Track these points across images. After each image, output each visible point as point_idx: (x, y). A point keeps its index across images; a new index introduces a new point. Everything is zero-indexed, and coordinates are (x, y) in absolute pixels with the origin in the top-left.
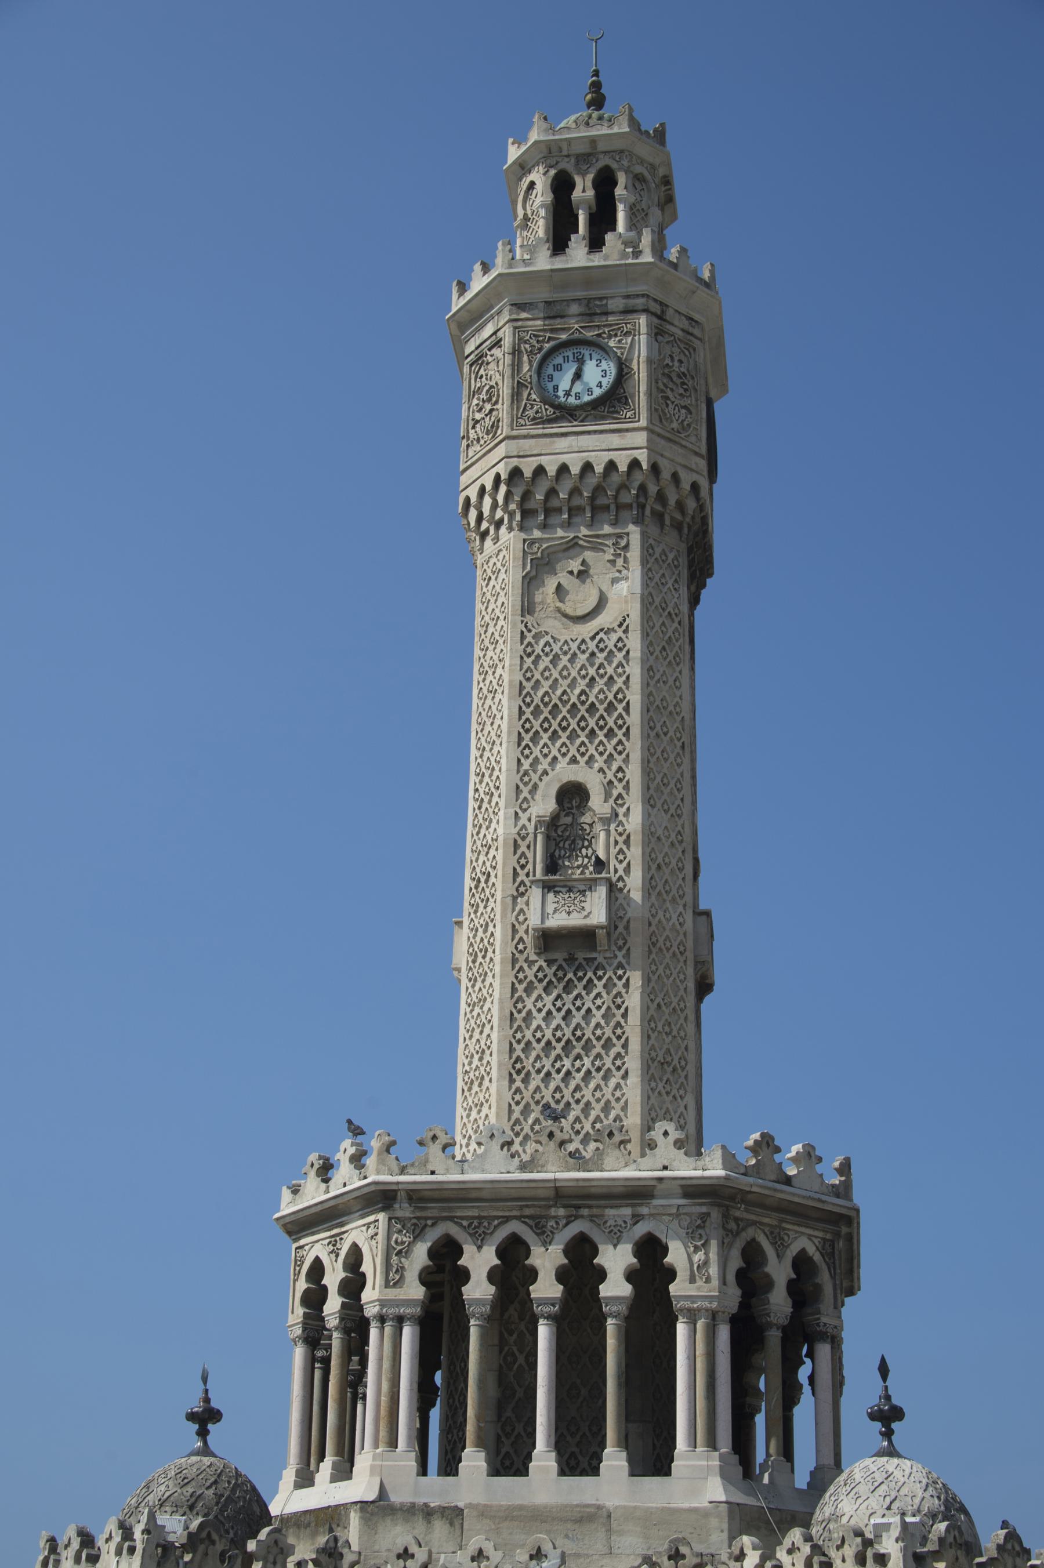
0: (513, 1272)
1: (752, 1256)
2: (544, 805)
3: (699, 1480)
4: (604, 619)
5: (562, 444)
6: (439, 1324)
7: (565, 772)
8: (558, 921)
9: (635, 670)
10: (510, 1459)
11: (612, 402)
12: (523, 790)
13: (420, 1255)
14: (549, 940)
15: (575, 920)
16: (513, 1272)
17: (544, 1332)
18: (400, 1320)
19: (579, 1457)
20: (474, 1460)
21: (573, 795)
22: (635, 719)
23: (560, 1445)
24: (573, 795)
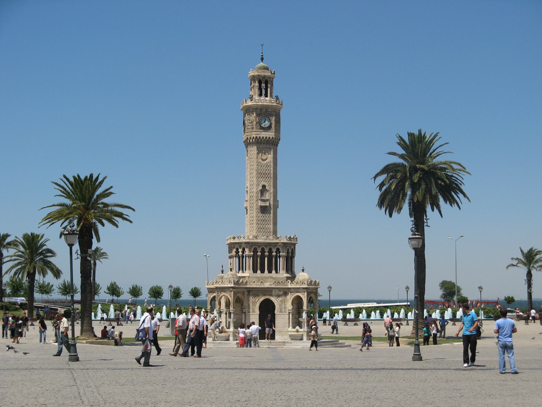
0: (263, 251)
1: (288, 250)
2: (260, 188)
3: (283, 274)
4: (267, 161)
5: (263, 133)
6: (254, 257)
7: (263, 183)
8: (263, 204)
9: (272, 168)
10: (263, 271)
11: (270, 127)
12: (258, 185)
13: (252, 249)
14: (261, 207)
15: (265, 205)
16: (263, 251)
17: (266, 259)
18: (250, 257)
19: (270, 271)
20: (259, 272)
21: (264, 186)
22: (272, 176)
23: (268, 270)
24: (264, 186)
